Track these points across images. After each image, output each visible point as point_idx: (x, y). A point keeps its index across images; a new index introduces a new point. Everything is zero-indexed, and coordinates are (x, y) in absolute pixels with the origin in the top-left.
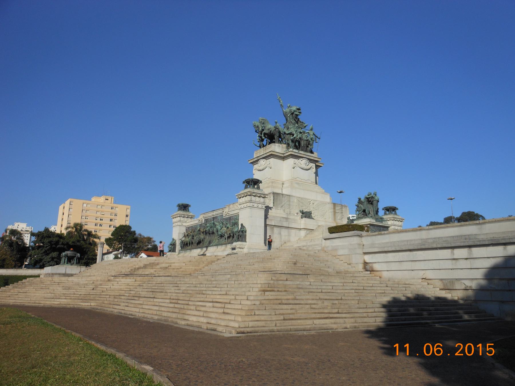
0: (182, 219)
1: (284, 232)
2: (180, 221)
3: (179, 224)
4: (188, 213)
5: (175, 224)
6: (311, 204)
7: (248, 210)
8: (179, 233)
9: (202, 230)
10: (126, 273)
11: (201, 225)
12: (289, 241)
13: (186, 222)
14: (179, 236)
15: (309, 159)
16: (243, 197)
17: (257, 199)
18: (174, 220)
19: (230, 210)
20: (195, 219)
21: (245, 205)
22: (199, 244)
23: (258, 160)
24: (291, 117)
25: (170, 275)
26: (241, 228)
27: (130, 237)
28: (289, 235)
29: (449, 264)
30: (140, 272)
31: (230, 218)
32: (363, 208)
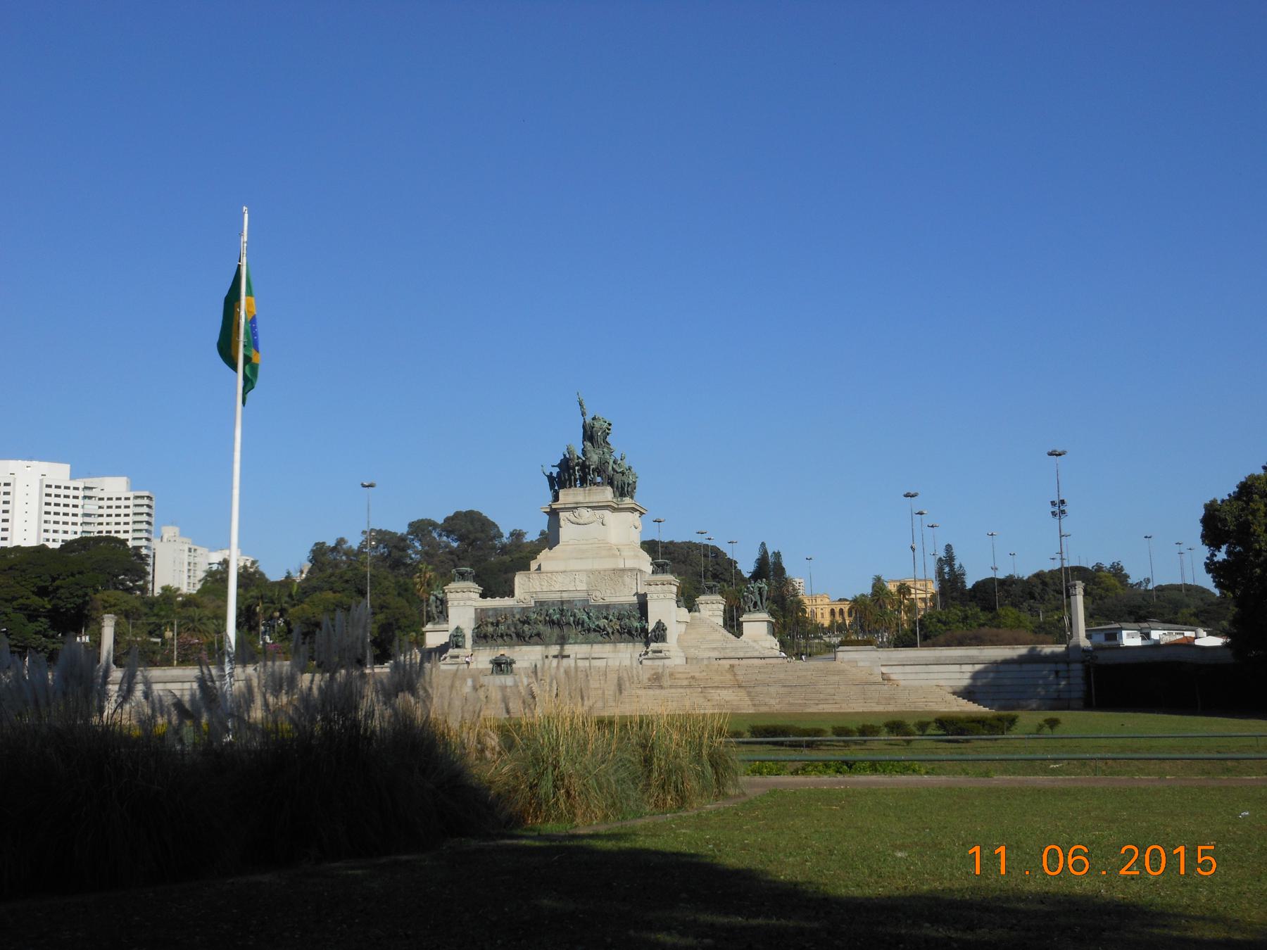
29: (958, 676)
31: (607, 607)
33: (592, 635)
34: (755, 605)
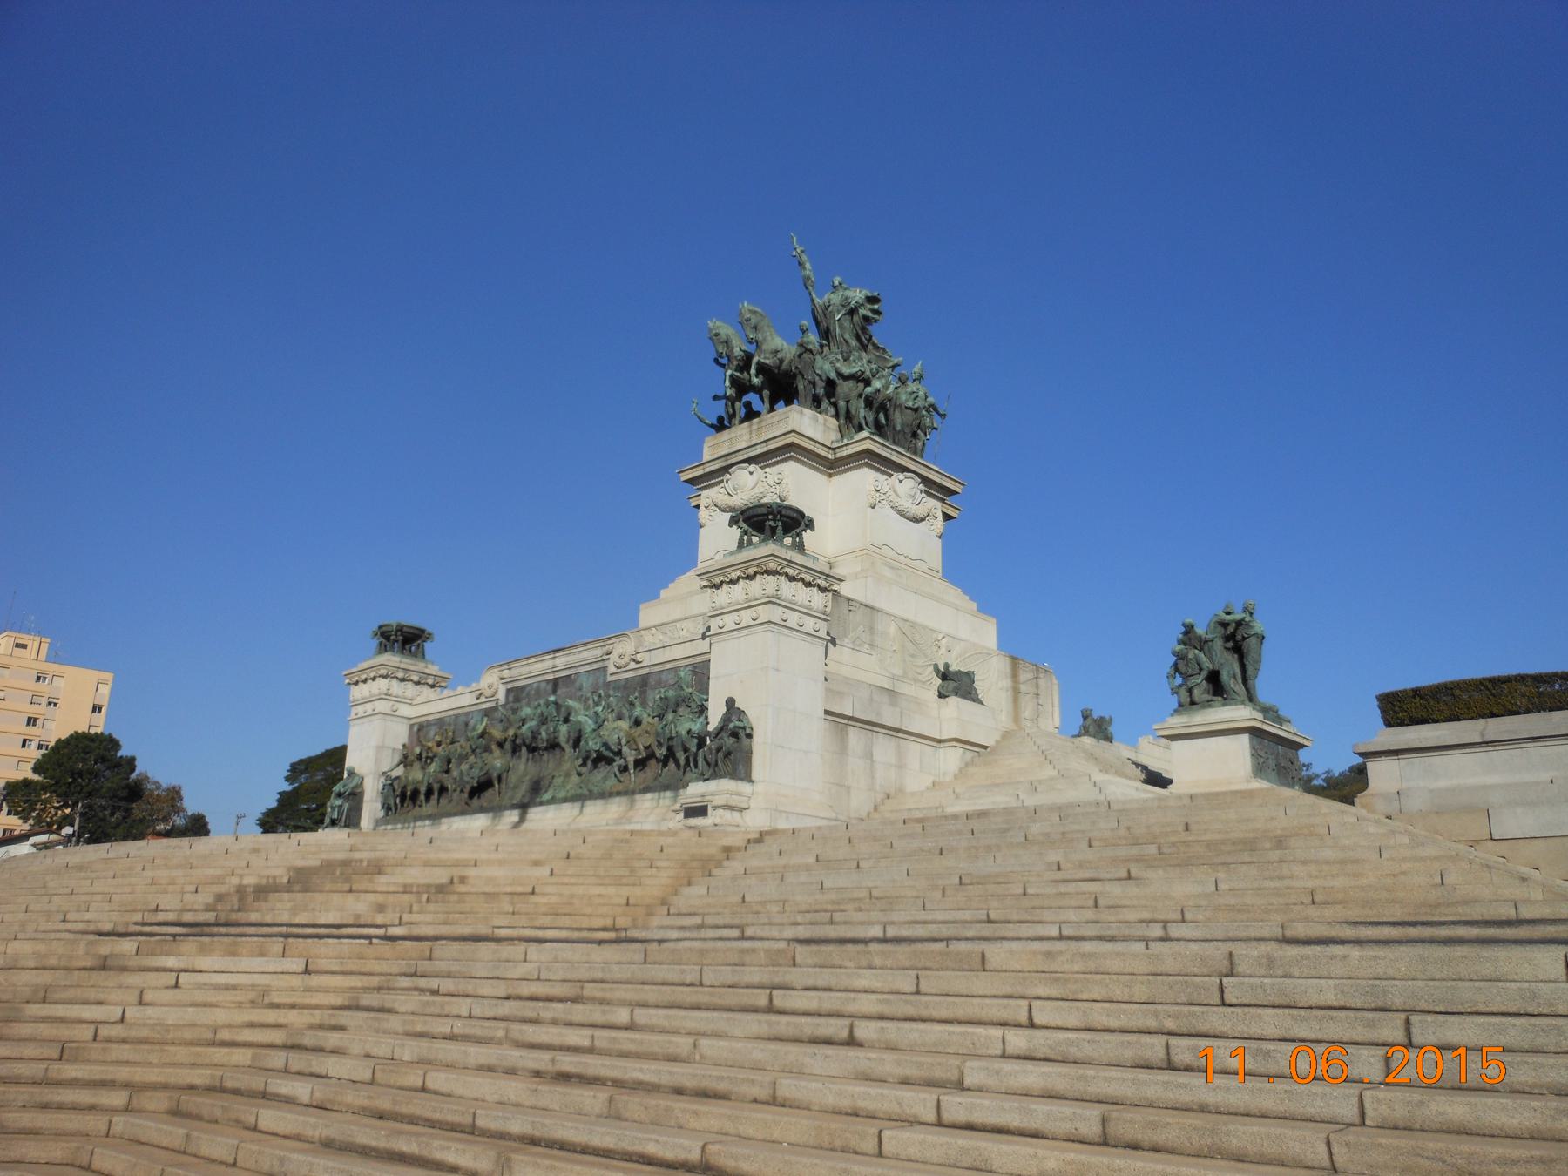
0: (396, 688)
1: (884, 748)
2: (387, 696)
3: (382, 706)
4: (421, 666)
5: (360, 710)
6: (943, 650)
7: (763, 637)
8: (380, 748)
9: (497, 733)
10: (188, 917)
11: (487, 713)
12: (901, 790)
13: (411, 702)
14: (377, 761)
15: (925, 481)
16: (733, 582)
17: (801, 594)
18: (357, 692)
19: (646, 646)
20: (460, 689)
21: (746, 617)
22: (480, 793)
23: (725, 470)
24: (847, 324)
25: (483, 930)
26: (726, 719)
27: (109, 781)
28: (901, 766)
30: (281, 909)
31: (643, 682)
32: (1207, 665)
33: (603, 770)
34: (1214, 678)
